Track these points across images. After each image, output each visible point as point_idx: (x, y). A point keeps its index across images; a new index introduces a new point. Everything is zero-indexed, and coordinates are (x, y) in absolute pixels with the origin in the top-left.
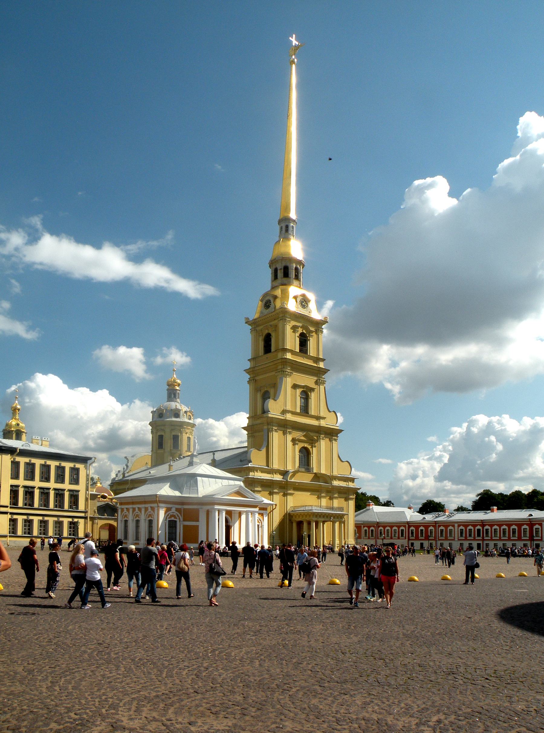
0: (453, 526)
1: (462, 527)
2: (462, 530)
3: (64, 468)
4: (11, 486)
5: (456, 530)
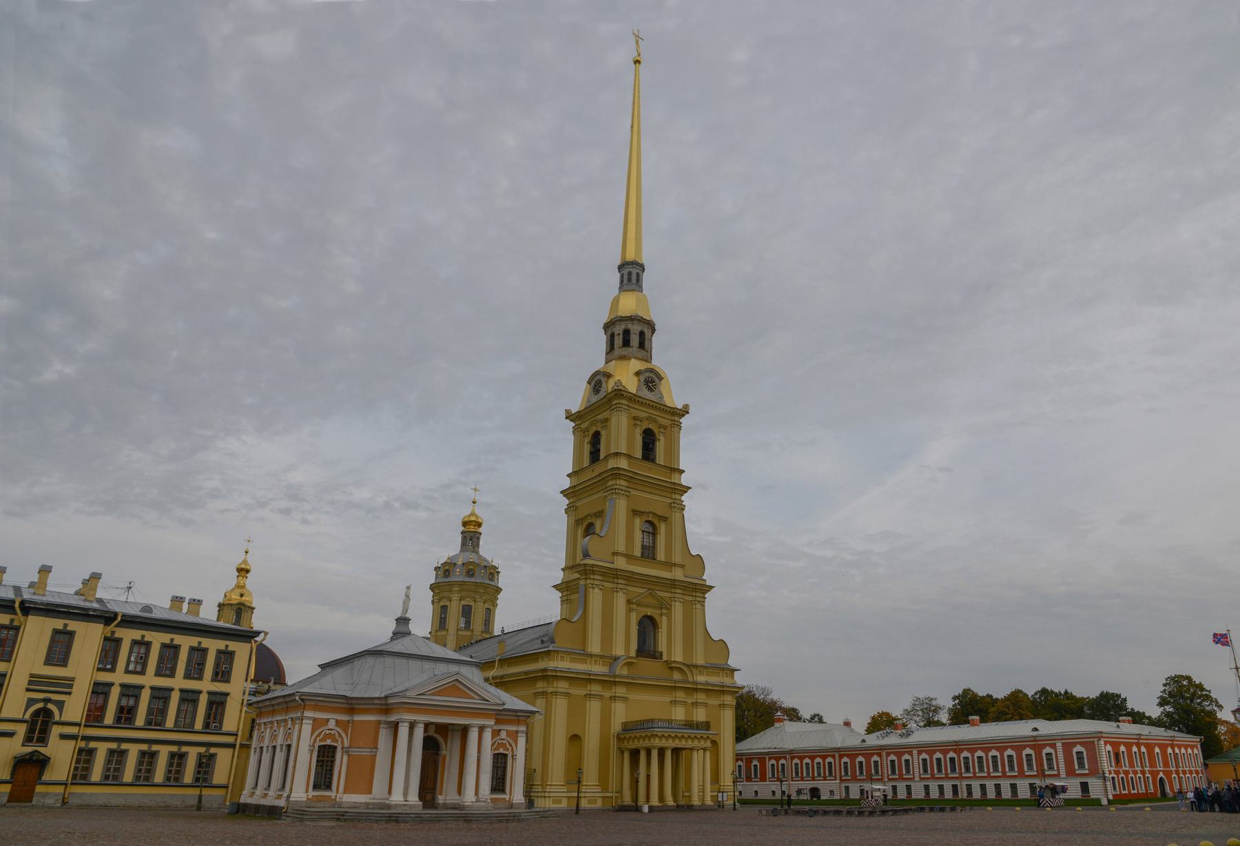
0: (911, 753)
1: (924, 756)
2: (924, 760)
4: (96, 684)
5: (916, 761)
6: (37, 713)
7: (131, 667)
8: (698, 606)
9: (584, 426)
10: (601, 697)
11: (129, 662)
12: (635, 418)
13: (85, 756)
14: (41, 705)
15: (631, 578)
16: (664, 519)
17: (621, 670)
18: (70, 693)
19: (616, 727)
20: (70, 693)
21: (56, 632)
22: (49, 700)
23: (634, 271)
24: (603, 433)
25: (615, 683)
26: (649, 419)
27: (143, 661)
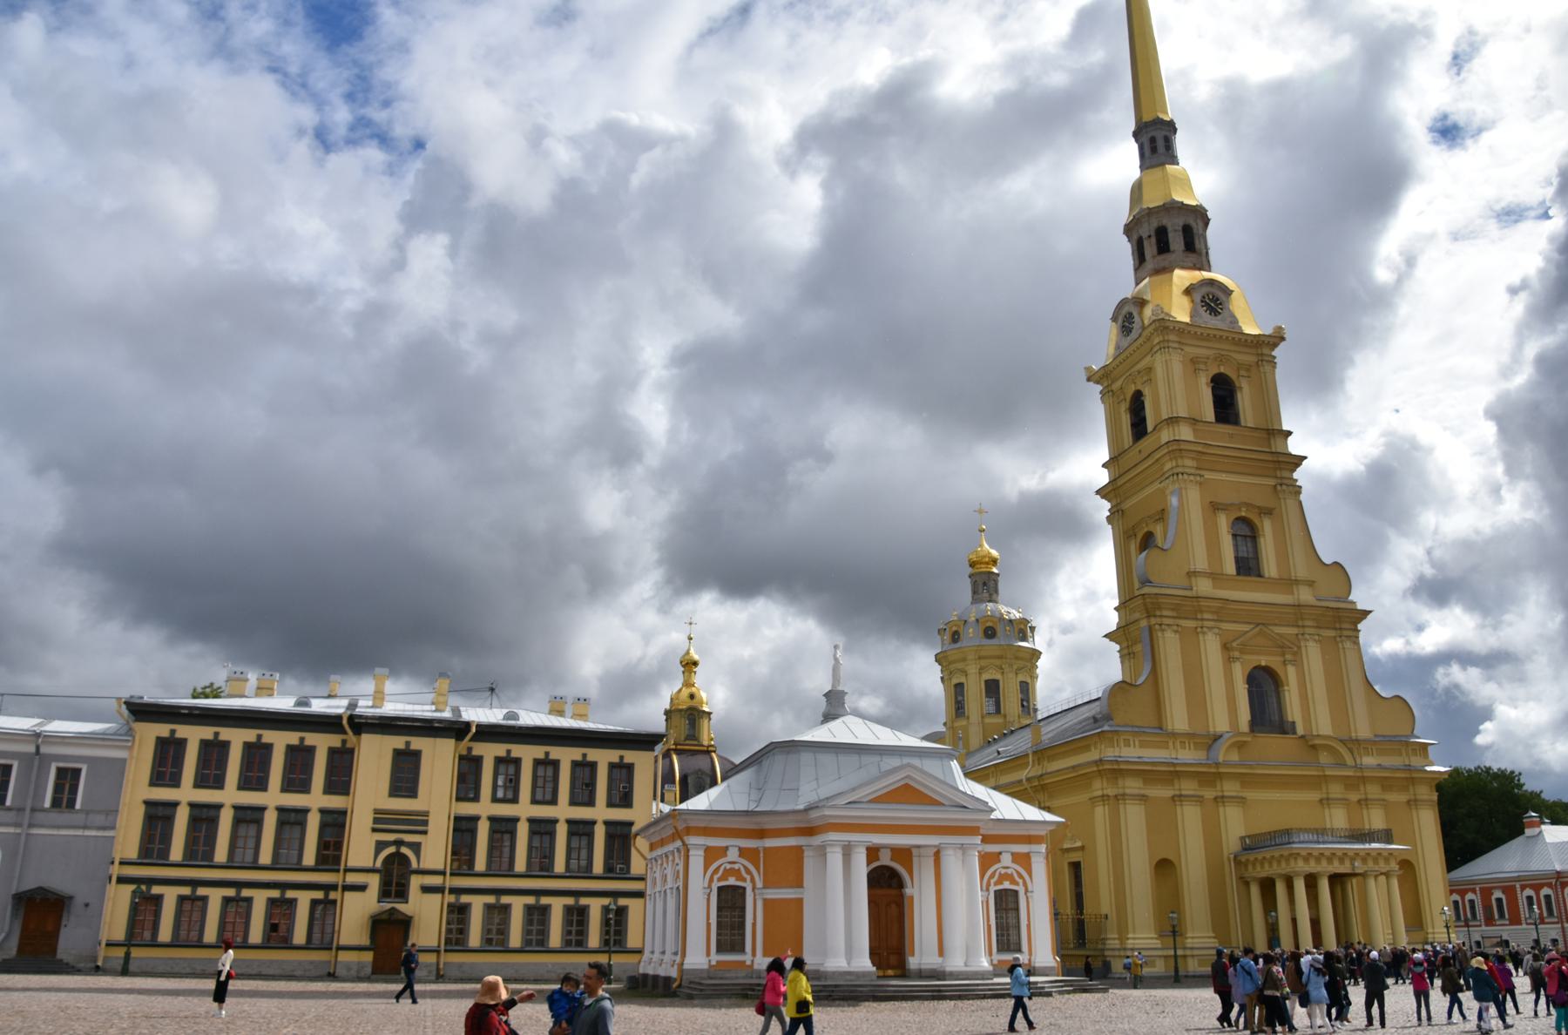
3: (593, 766)
7: (500, 794)
8: (1348, 645)
9: (1116, 386)
10: (1199, 800)
11: (495, 787)
12: (1194, 361)
13: (459, 913)
14: (392, 849)
15: (1224, 611)
16: (1268, 512)
17: (1222, 753)
18: (425, 833)
19: (1231, 843)
20: (425, 833)
21: (398, 754)
23: (1159, 135)
24: (1146, 391)
25: (1220, 776)
26: (1220, 359)
27: (514, 783)
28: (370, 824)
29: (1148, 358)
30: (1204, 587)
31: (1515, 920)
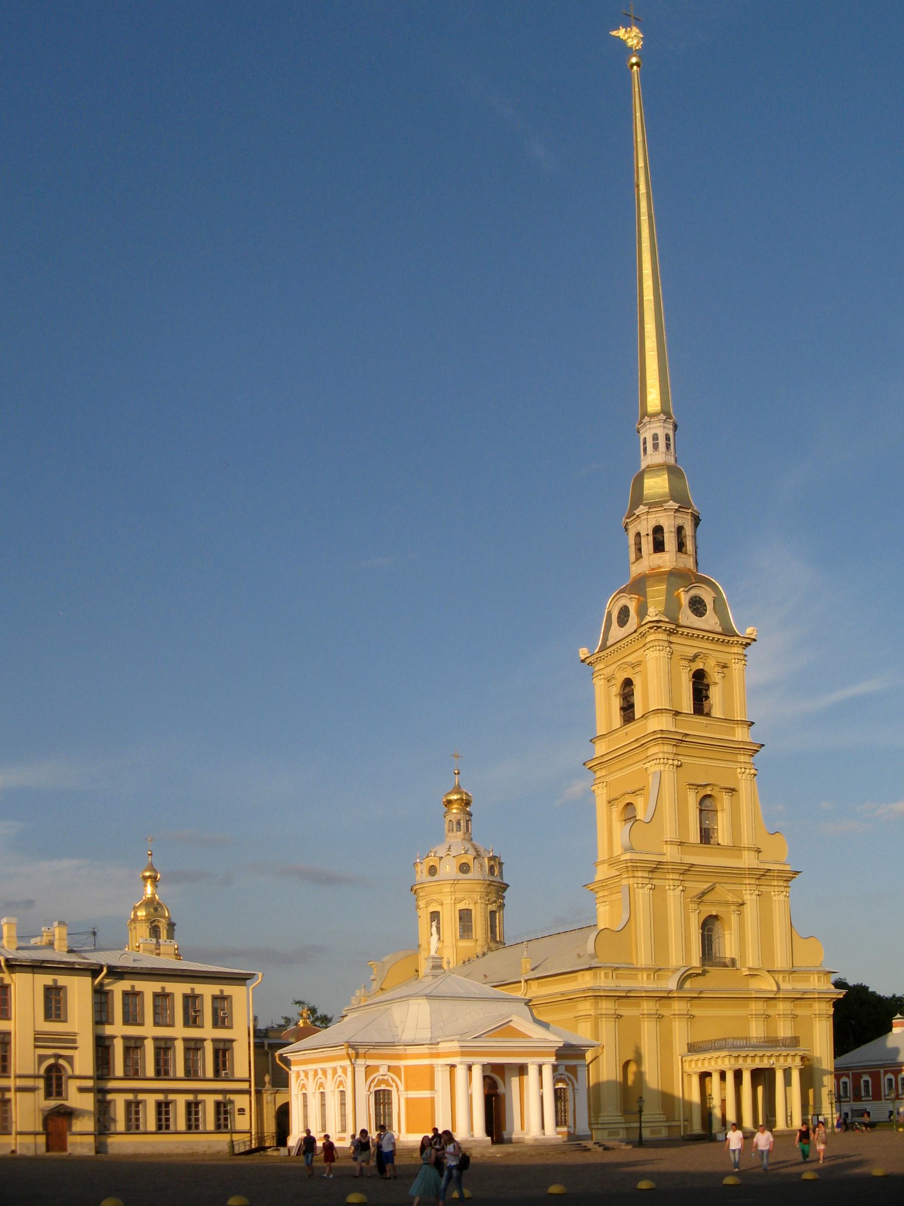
6: (49, 1069)
18: (76, 1048)
22: (59, 1056)
28: (31, 1042)
29: (641, 652)
30: (671, 854)
31: (877, 1096)
